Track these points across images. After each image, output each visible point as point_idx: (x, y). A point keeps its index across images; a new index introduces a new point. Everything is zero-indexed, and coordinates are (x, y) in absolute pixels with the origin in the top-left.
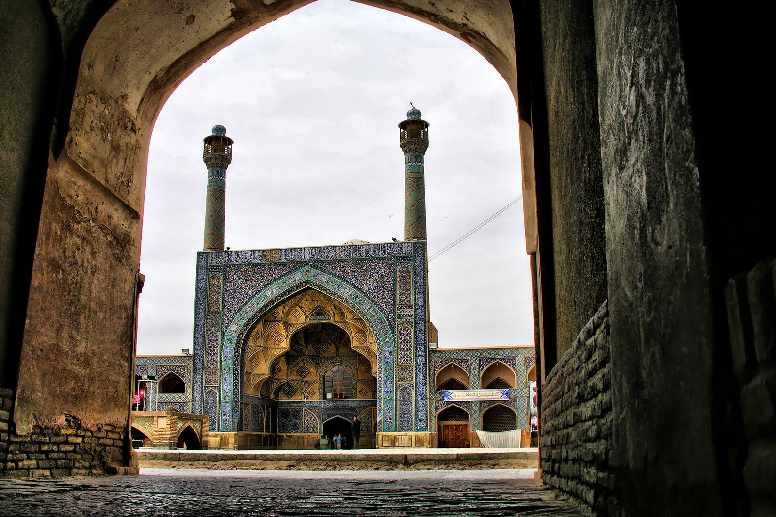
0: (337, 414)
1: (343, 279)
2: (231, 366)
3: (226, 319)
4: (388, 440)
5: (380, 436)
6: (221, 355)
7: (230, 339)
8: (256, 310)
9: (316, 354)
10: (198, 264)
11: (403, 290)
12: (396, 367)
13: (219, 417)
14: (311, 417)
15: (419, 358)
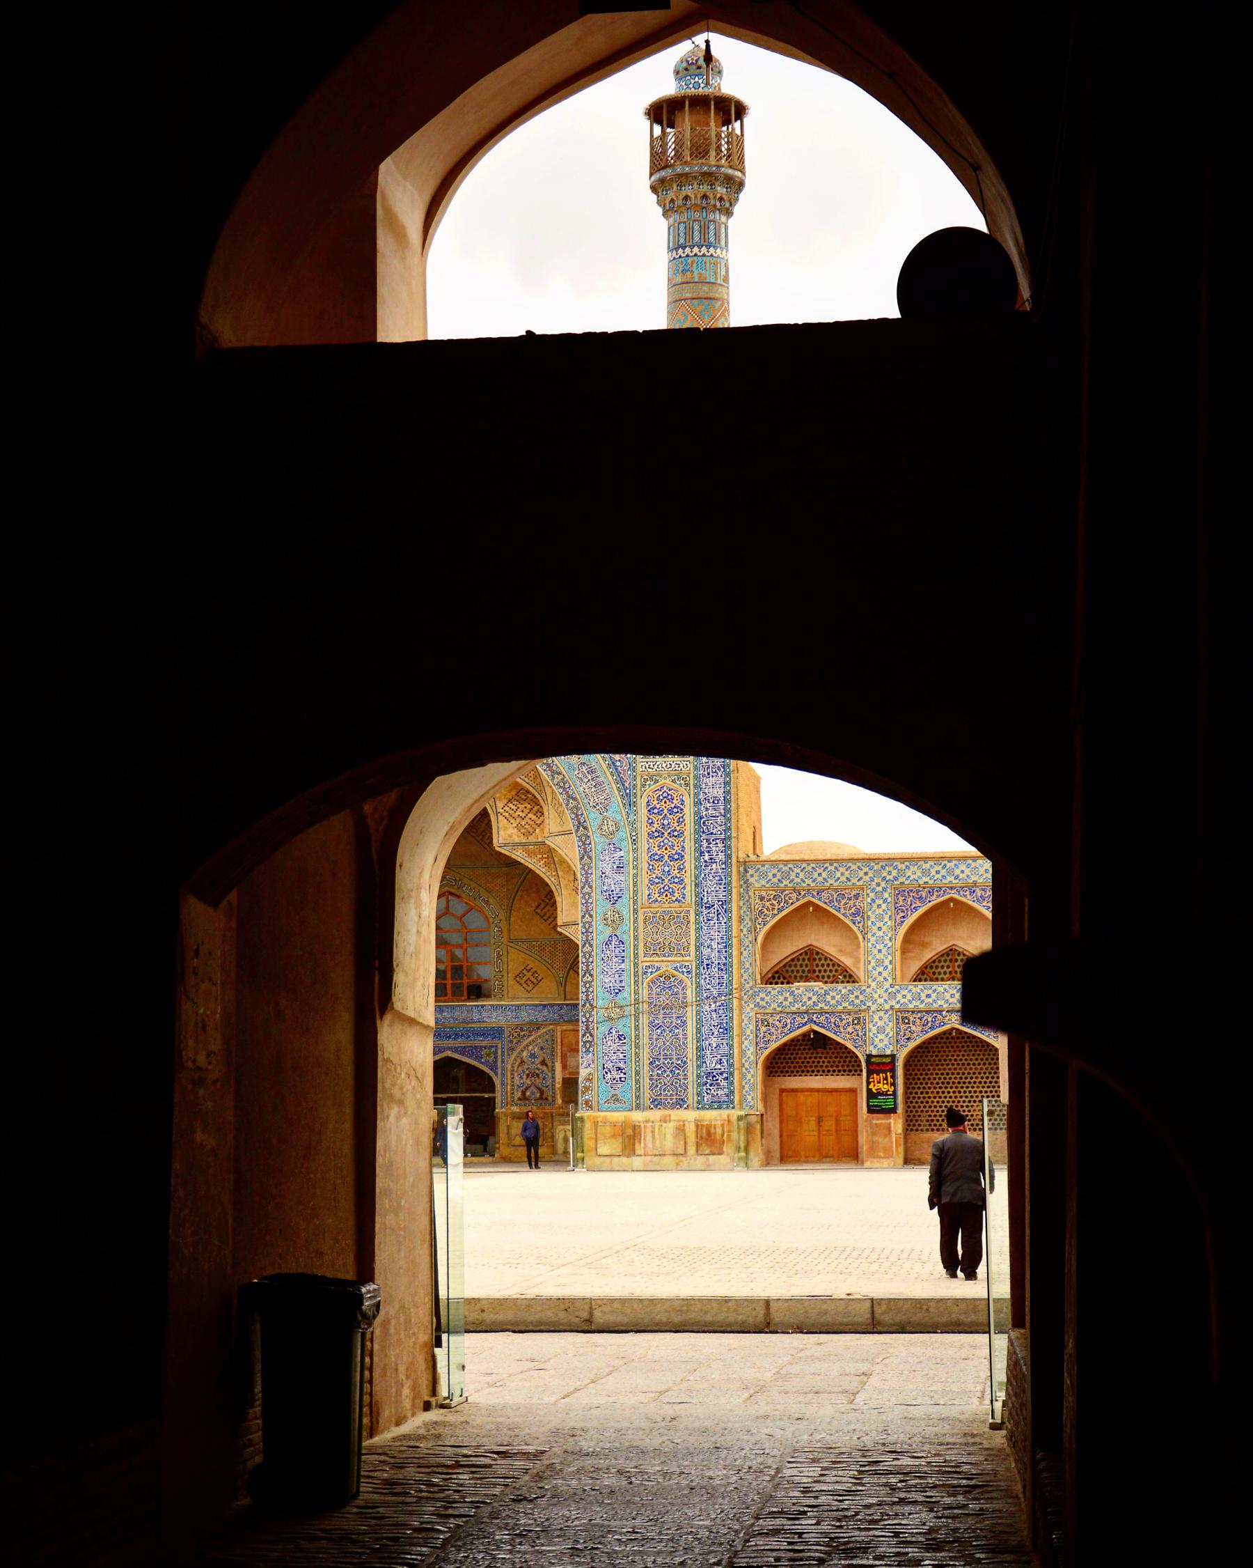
5: (588, 1126)
15: (711, 885)
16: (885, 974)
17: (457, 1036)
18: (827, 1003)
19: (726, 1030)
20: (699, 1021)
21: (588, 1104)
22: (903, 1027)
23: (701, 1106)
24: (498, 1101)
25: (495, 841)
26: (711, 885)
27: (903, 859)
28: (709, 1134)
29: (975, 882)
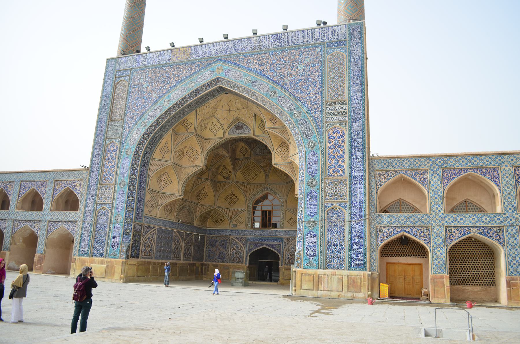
0: (263, 244)
1: (260, 73)
2: (127, 180)
3: (127, 127)
4: (310, 281)
5: (299, 275)
6: (117, 168)
7: (129, 150)
8: (159, 115)
9: (245, 181)
10: (106, 71)
11: (334, 82)
12: (322, 180)
13: (108, 239)
14: (237, 247)
15: (356, 168)
16: (439, 209)
17: (268, 240)
18: (411, 222)
19: (363, 233)
20: (350, 229)
21: (299, 266)
22: (449, 234)
23: (350, 269)
24: (280, 264)
25: (273, 163)
26: (356, 168)
27: (446, 156)
28: (354, 282)
29: (482, 166)
